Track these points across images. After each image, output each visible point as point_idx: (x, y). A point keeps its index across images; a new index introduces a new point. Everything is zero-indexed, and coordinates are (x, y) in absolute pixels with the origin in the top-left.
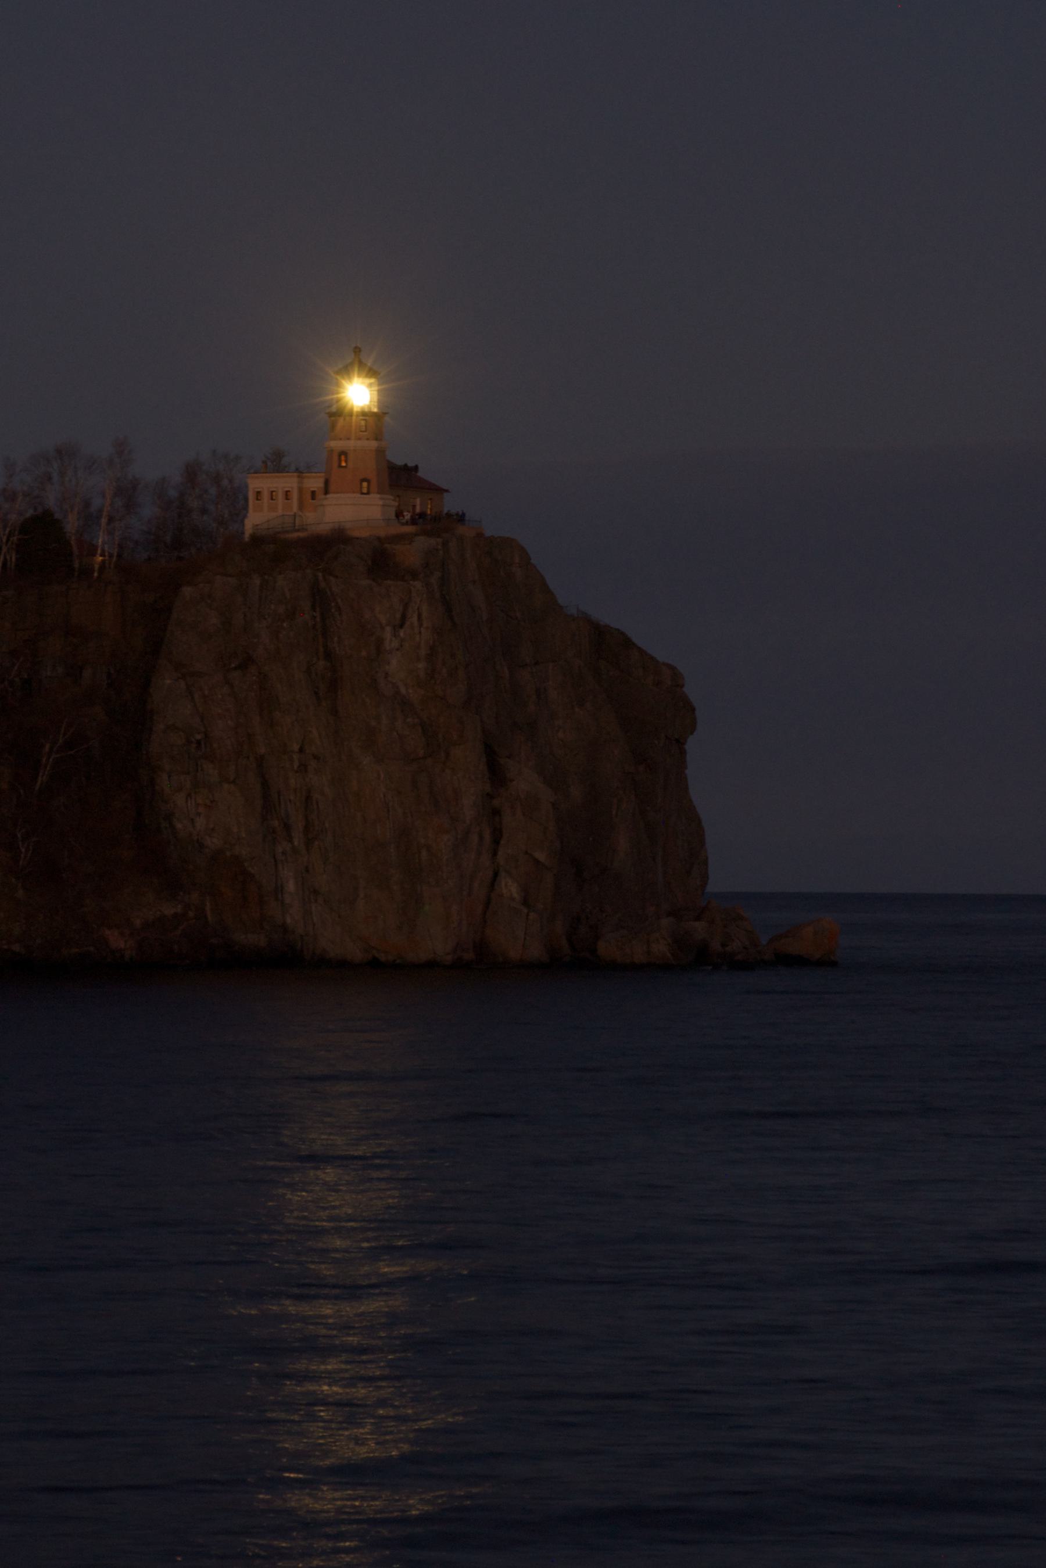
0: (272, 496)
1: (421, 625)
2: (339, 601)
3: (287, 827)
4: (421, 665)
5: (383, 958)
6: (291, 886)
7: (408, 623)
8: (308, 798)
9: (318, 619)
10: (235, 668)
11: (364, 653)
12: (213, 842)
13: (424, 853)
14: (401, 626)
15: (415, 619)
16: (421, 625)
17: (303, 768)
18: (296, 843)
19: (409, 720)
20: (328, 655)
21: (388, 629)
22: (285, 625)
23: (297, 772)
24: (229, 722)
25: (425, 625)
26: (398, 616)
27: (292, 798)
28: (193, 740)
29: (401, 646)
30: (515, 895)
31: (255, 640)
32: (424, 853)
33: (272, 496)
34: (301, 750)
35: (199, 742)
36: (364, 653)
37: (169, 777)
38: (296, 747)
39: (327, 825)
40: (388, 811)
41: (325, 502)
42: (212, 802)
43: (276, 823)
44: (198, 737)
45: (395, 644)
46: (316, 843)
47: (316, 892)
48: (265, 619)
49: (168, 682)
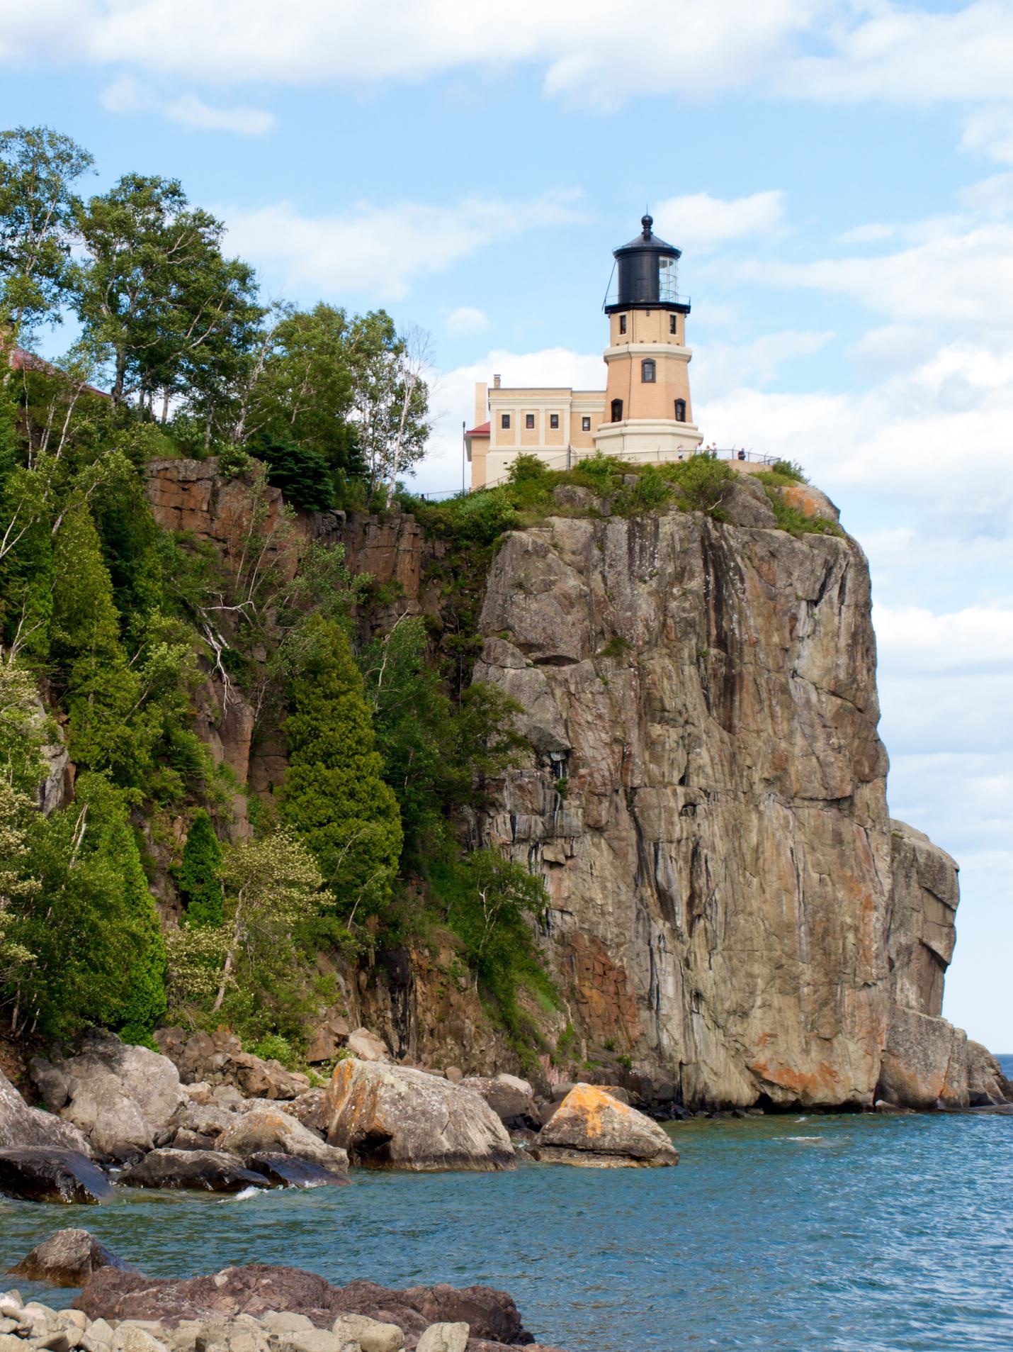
0: (530, 420)
1: (842, 603)
2: (739, 559)
4: (843, 660)
5: (778, 1096)
6: (669, 987)
7: (826, 597)
8: (695, 853)
9: (711, 587)
10: (607, 653)
11: (776, 639)
13: (851, 937)
14: (816, 603)
15: (834, 592)
16: (842, 603)
17: (690, 807)
18: (678, 923)
19: (834, 740)
20: (723, 642)
21: (804, 604)
22: (675, 591)
23: (681, 814)
24: (603, 735)
25: (848, 600)
26: (818, 587)
27: (673, 855)
28: (548, 761)
29: (814, 632)
30: (914, 1003)
31: (629, 614)
32: (851, 937)
33: (530, 420)
34: (682, 782)
35: (555, 766)
36: (776, 639)
37: (513, 819)
38: (676, 777)
39: (717, 896)
40: (798, 876)
41: (625, 430)
42: (567, 858)
43: (648, 892)
44: (557, 757)
45: (808, 629)
46: (702, 922)
47: (698, 996)
48: (645, 582)
49: (511, 672)
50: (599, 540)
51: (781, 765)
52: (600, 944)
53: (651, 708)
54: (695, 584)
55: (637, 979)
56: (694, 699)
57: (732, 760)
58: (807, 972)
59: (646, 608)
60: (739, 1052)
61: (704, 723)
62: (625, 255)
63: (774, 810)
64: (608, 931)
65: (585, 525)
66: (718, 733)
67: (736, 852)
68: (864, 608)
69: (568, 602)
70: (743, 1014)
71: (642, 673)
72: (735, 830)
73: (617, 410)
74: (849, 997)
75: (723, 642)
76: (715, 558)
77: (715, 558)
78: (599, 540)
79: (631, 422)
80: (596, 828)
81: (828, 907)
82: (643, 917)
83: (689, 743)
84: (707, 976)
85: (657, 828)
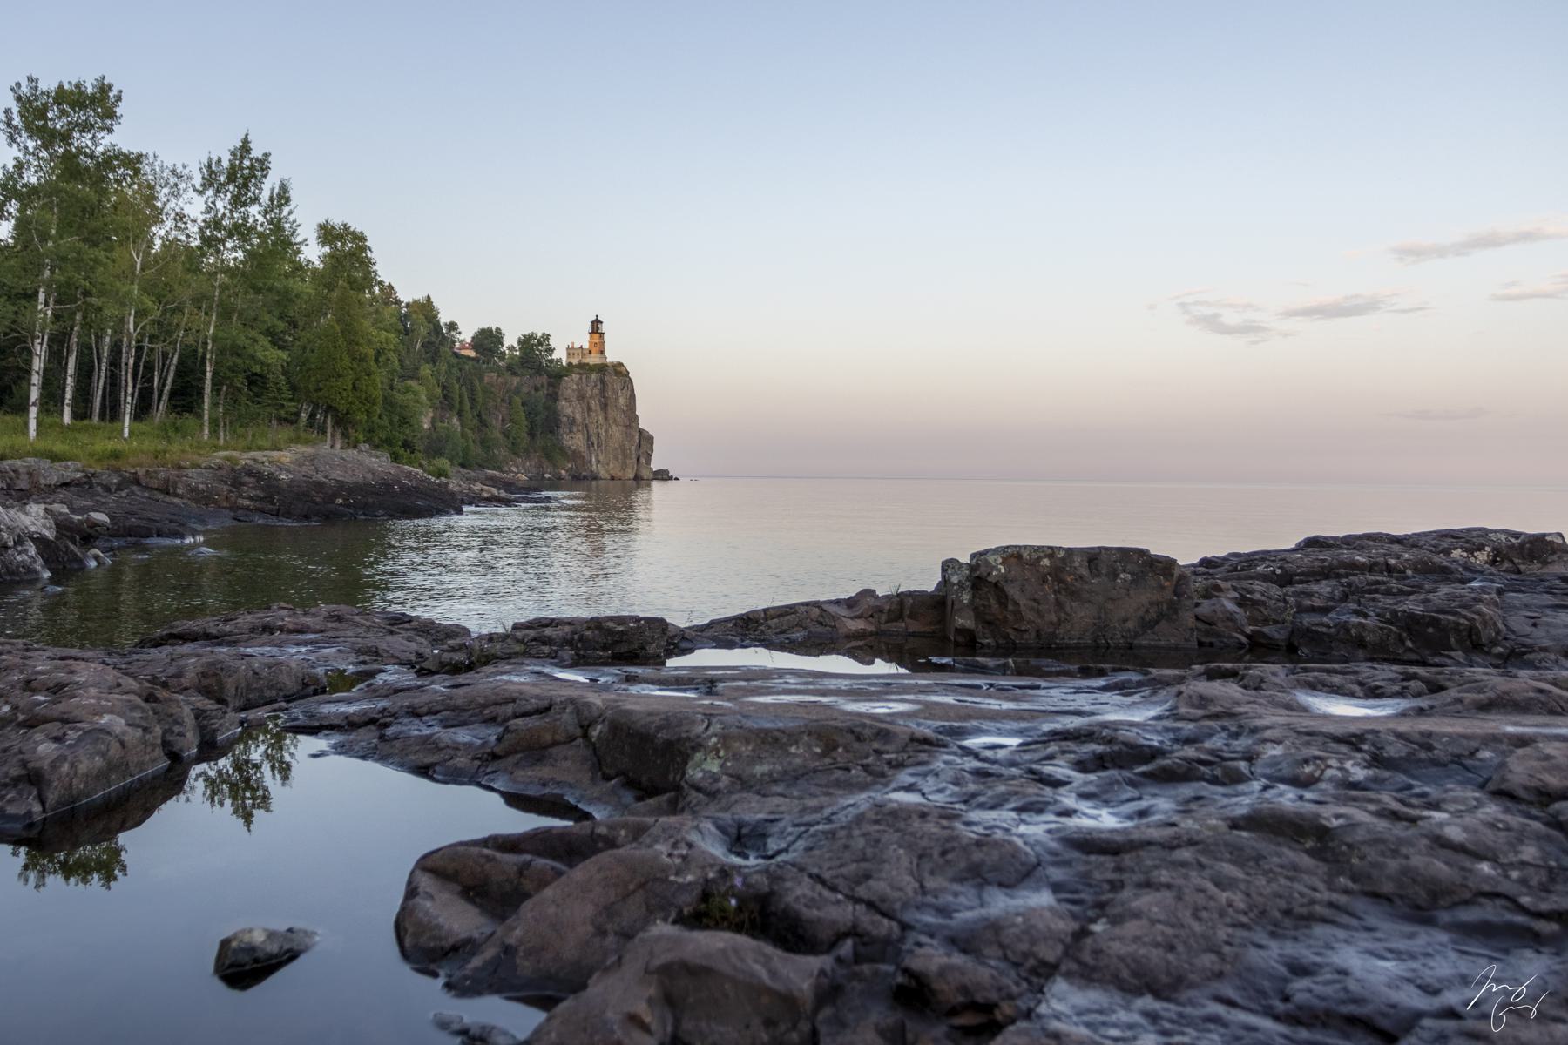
3: (593, 444)
12: (574, 448)
20: (604, 397)
50: (581, 378)
51: (615, 420)
52: (580, 452)
53: (589, 409)
54: (599, 387)
55: (587, 458)
56: (598, 408)
57: (606, 419)
58: (620, 457)
59: (589, 392)
60: (607, 471)
61: (599, 412)
62: (592, 323)
63: (614, 427)
64: (582, 450)
65: (578, 376)
66: (603, 414)
67: (607, 435)
68: (633, 391)
69: (573, 390)
70: (608, 464)
71: (588, 403)
72: (606, 431)
73: (590, 352)
74: (628, 461)
75: (604, 397)
76: (603, 382)
77: (603, 382)
78: (581, 378)
79: (592, 355)
80: (578, 430)
81: (624, 445)
82: (589, 447)
83: (597, 416)
84: (601, 458)
85: (591, 431)
